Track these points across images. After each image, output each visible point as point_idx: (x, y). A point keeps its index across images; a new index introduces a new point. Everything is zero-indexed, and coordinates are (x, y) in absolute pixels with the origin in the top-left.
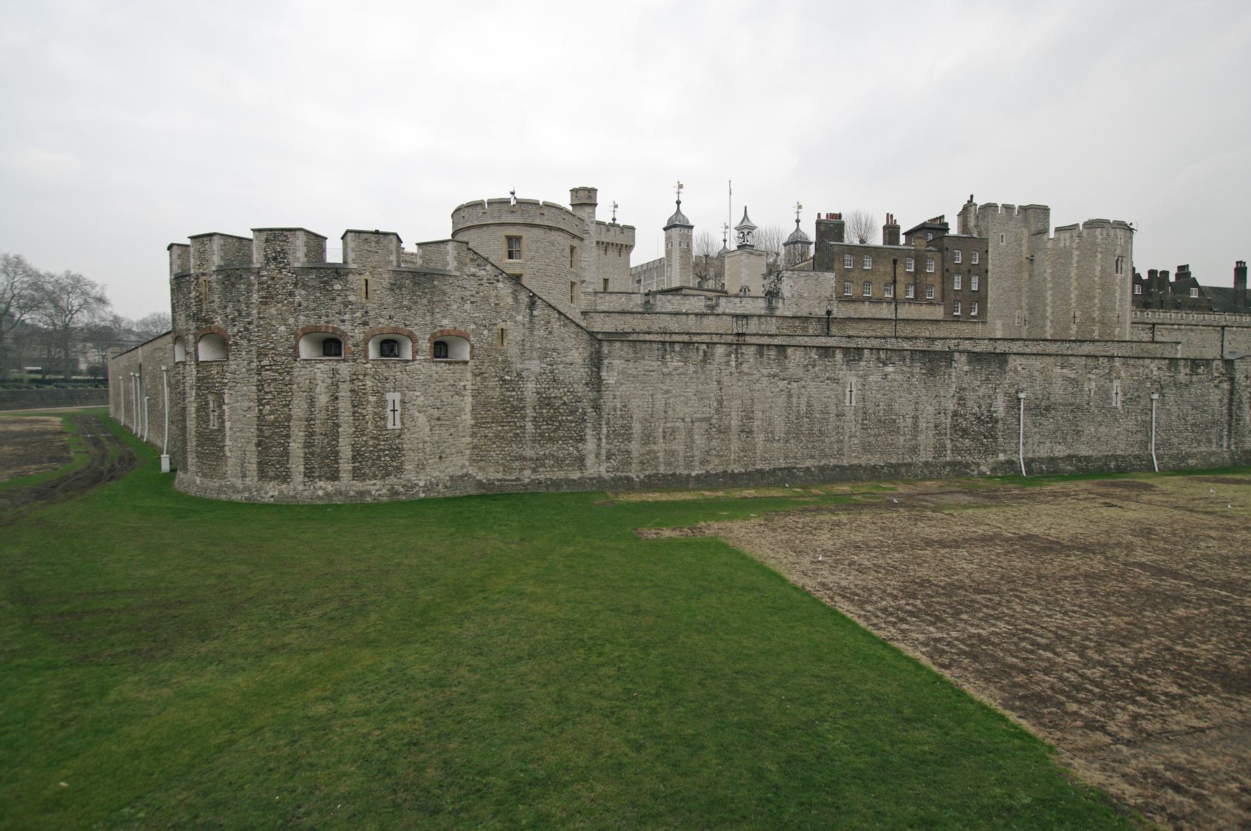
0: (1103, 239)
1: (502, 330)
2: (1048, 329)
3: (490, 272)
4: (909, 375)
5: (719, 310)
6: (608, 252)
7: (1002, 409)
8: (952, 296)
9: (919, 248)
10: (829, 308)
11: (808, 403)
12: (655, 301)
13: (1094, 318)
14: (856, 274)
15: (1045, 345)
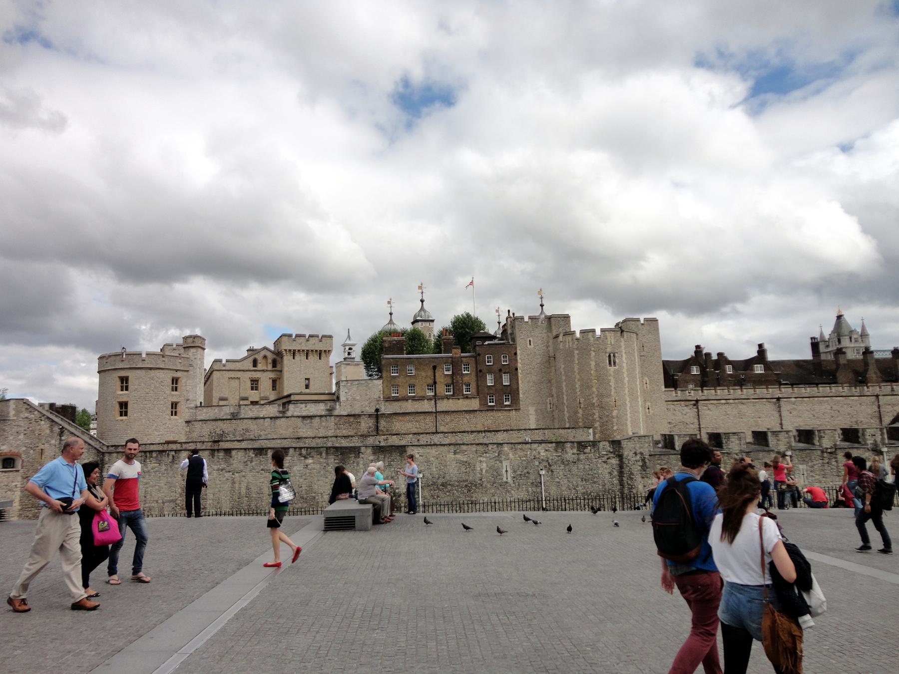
0: (594, 341)
1: (42, 449)
2: (566, 412)
3: (37, 415)
4: (325, 465)
5: (289, 414)
6: (309, 358)
7: (404, 486)
8: (486, 390)
9: (454, 356)
10: (378, 407)
11: (247, 487)
12: (240, 410)
13: (594, 404)
14: (400, 381)
15: (462, 435)
